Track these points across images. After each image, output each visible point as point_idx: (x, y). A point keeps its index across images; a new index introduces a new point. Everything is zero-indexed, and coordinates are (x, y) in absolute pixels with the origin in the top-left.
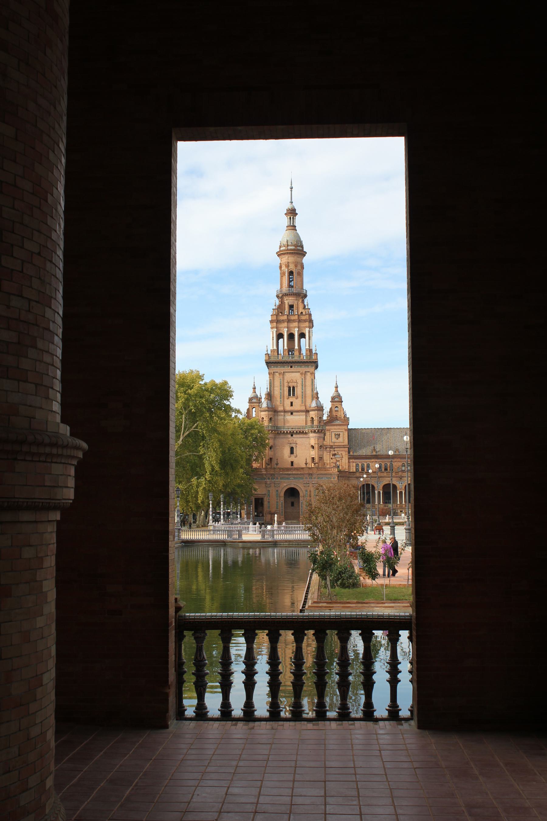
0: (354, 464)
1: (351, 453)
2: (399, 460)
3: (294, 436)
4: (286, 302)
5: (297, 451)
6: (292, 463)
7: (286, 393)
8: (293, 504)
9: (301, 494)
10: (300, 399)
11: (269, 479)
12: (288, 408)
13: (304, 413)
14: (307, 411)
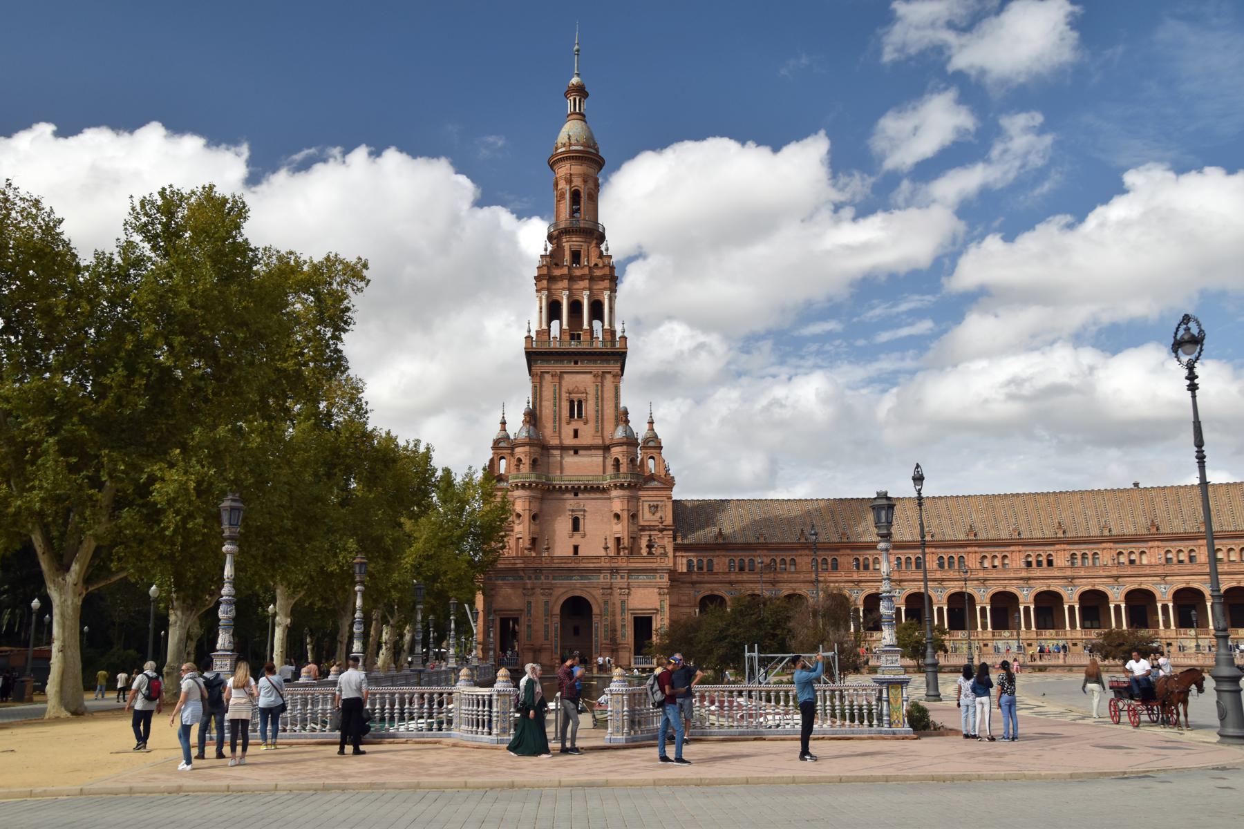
0: (685, 561)
1: (679, 541)
2: (765, 552)
3: (580, 495)
4: (566, 246)
5: (587, 525)
6: (576, 548)
7: (565, 412)
8: (576, 631)
9: (596, 610)
10: (592, 424)
11: (530, 578)
12: (569, 441)
13: (601, 452)
14: (606, 448)
